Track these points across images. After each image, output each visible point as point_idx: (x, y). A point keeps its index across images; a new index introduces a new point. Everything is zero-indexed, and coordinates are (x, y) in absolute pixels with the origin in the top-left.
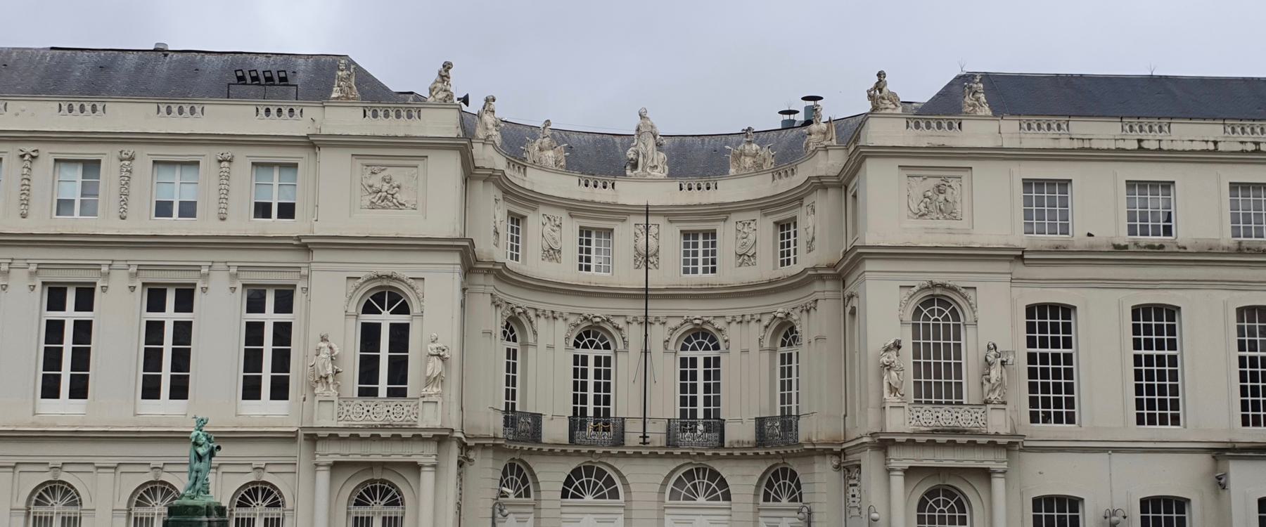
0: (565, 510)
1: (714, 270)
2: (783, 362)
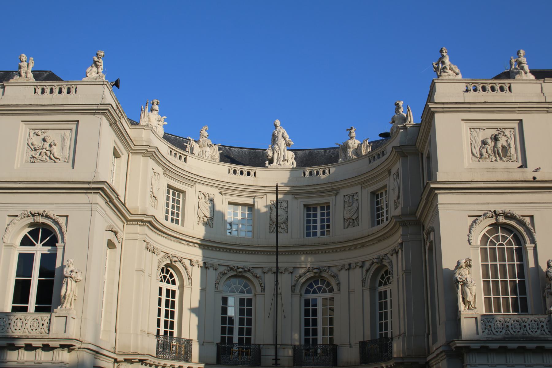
2: (380, 298)
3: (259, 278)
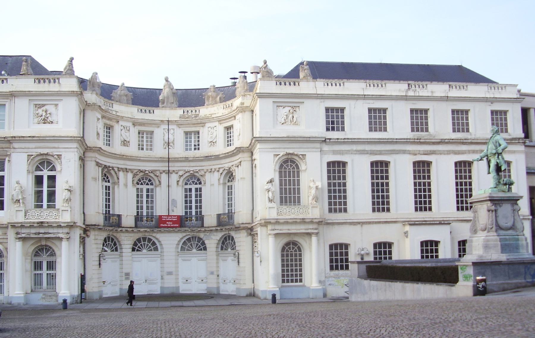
0: (134, 256)
1: (199, 149)
3: (158, 176)
